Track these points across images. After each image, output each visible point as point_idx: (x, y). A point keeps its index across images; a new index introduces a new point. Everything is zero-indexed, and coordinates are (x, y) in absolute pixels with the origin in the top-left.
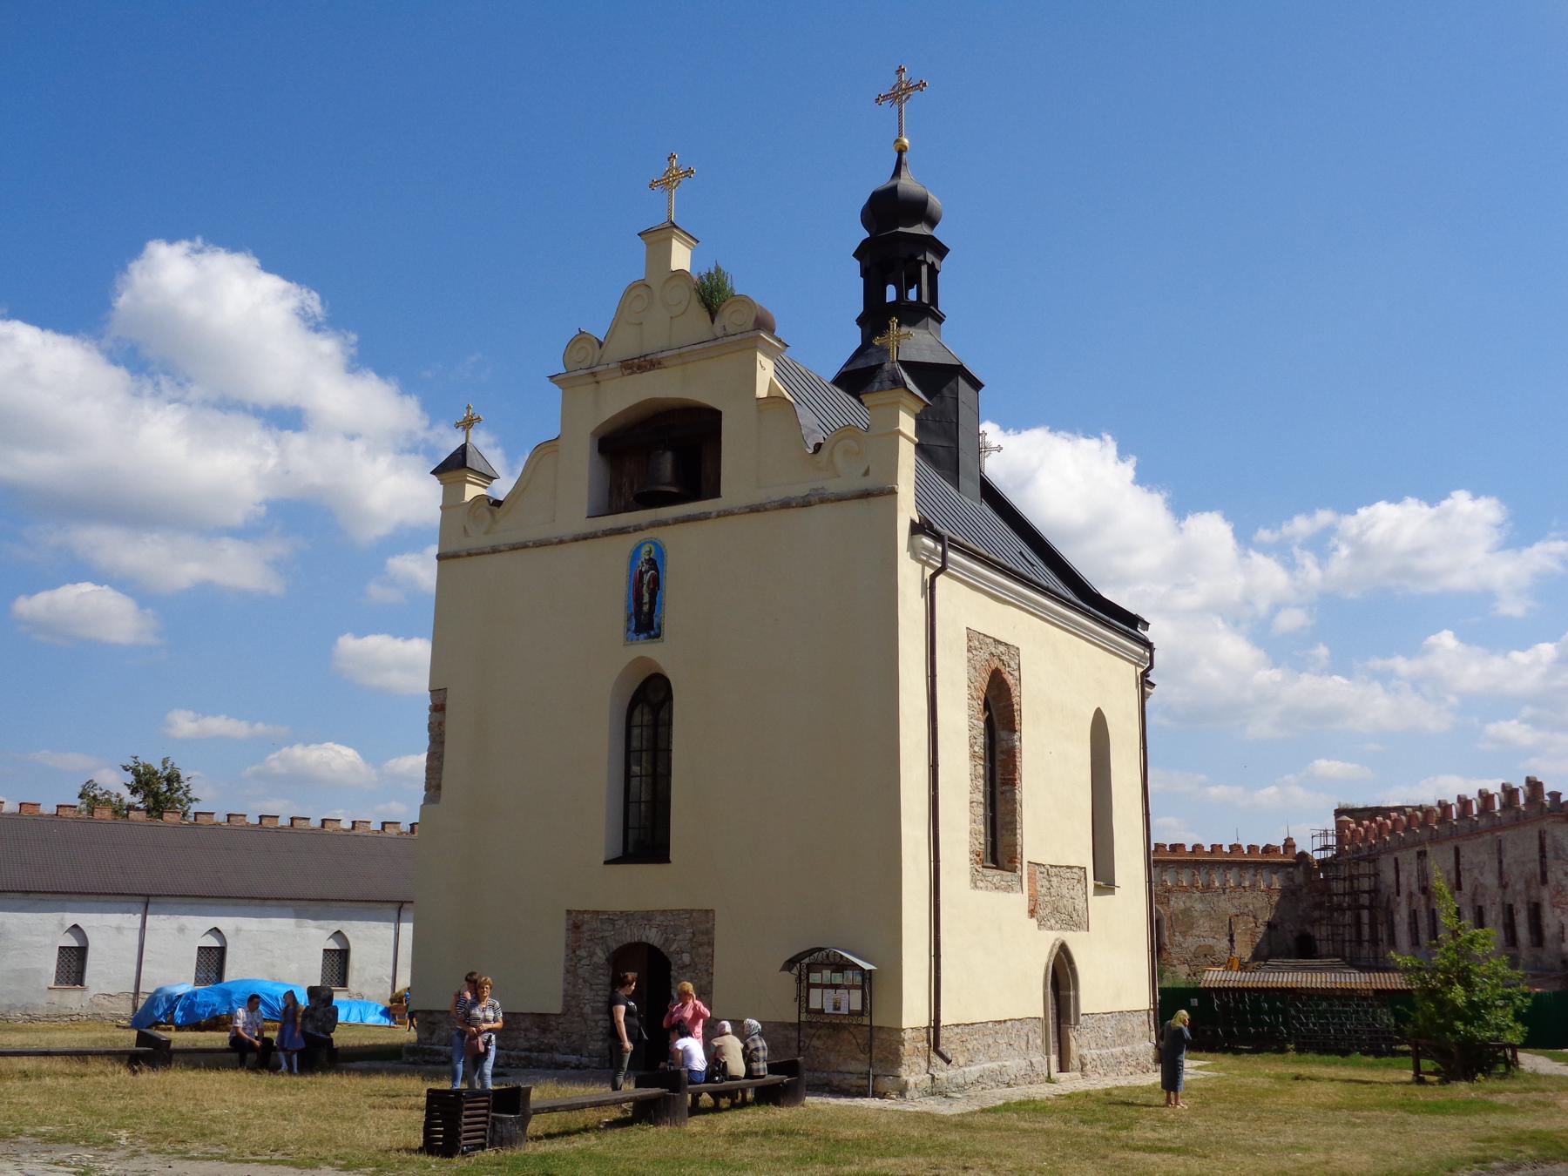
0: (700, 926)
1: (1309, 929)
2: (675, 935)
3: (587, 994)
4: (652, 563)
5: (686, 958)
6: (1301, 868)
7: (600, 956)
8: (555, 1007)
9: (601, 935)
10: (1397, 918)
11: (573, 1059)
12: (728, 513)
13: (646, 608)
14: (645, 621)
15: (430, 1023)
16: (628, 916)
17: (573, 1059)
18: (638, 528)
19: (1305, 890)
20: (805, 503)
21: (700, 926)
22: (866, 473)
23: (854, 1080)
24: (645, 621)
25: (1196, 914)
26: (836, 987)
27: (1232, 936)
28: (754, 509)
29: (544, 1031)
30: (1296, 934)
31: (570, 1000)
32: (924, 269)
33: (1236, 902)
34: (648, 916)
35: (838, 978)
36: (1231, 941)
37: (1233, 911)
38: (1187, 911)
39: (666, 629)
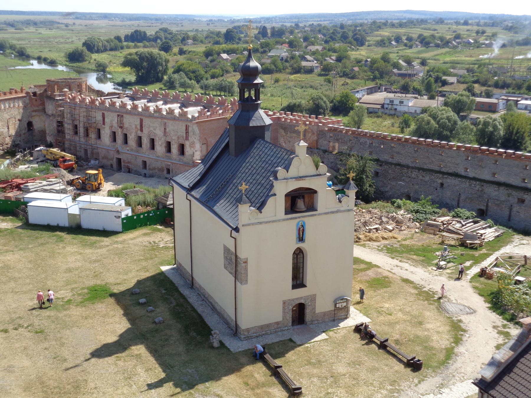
0: (313, 298)
1: (31, 120)
3: (288, 315)
4: (302, 226)
5: (310, 304)
6: (28, 98)
7: (291, 307)
8: (281, 319)
10: (102, 132)
11: (286, 328)
12: (320, 214)
13: (301, 236)
14: (301, 239)
16: (297, 299)
17: (286, 328)
18: (299, 217)
19: (29, 105)
20: (337, 212)
21: (313, 298)
22: (348, 206)
23: (343, 317)
24: (301, 239)
26: (341, 303)
27: (8, 126)
28: (326, 213)
29: (278, 325)
30: (27, 122)
31: (284, 317)
33: (9, 114)
34: (301, 298)
35: (342, 301)
36: (8, 128)
37: (8, 117)
39: (306, 241)
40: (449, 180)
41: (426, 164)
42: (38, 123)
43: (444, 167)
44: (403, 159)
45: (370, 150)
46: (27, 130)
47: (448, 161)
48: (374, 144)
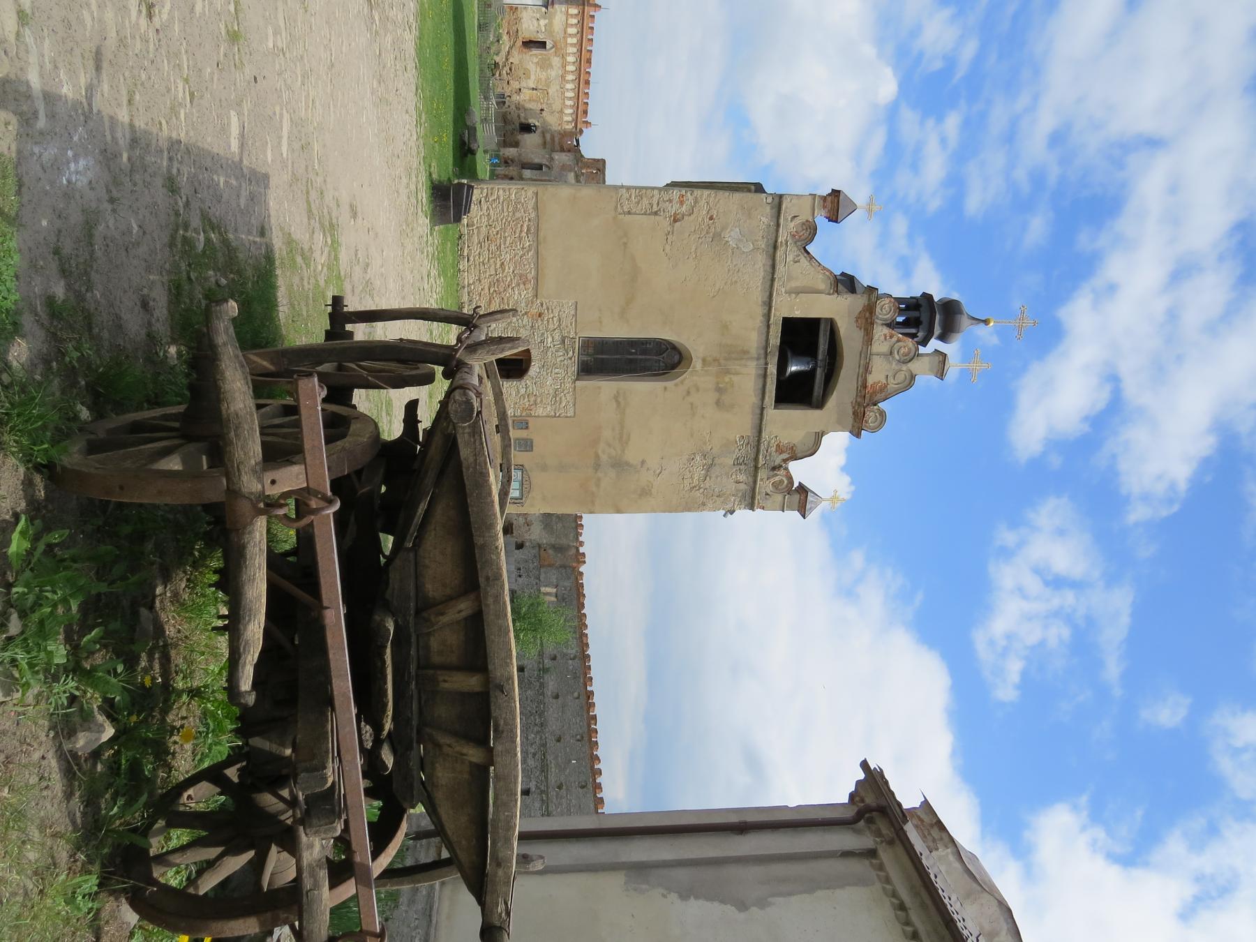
1: (539, 131)
2: (535, 384)
7: (523, 333)
9: (536, 334)
15: (480, 202)
25: (549, 71)
27: (536, 89)
32: (913, 331)
33: (556, 94)
36: (533, 89)
38: (551, 66)
40: (537, 805)
41: (556, 758)
42: (530, 140)
43: (557, 794)
44: (555, 715)
45: (558, 655)
46: (523, 121)
47: (571, 800)
48: (570, 661)
